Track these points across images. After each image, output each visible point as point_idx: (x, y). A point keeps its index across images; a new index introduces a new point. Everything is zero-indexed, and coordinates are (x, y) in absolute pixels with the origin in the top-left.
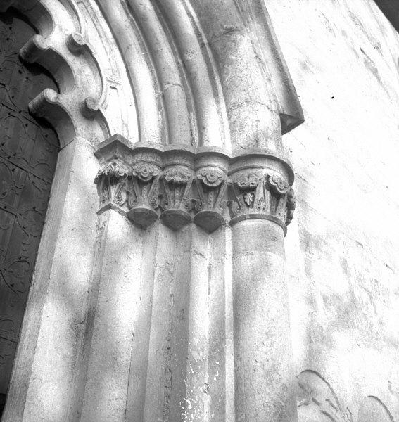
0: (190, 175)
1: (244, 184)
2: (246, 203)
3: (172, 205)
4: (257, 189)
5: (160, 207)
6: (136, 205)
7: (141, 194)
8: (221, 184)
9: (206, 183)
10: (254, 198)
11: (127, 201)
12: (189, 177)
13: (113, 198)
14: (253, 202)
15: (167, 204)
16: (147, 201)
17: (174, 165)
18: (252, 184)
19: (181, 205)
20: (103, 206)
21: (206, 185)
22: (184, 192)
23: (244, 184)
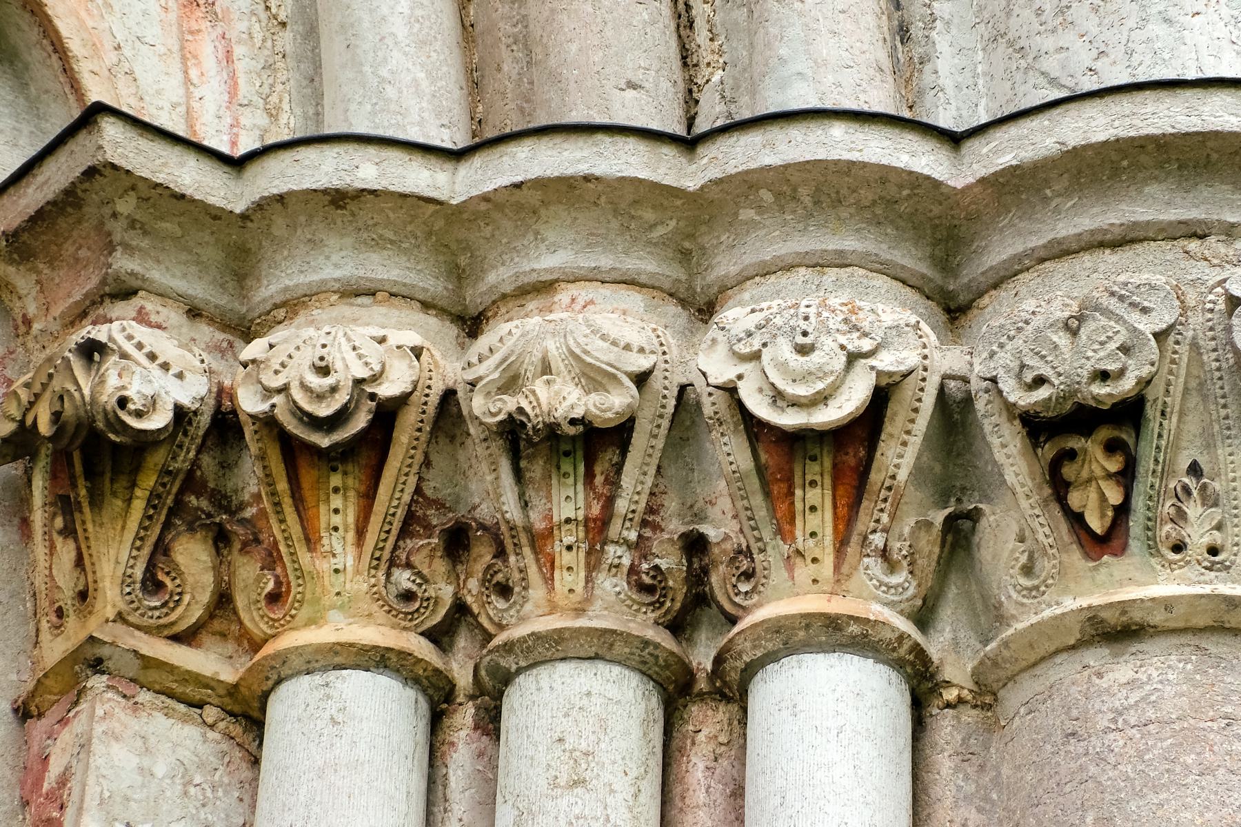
0: (643, 363)
1: (1040, 381)
2: (1076, 520)
3: (537, 592)
4: (1151, 412)
5: (460, 609)
6: (289, 623)
7: (311, 542)
8: (881, 397)
9: (760, 407)
10: (1127, 477)
11: (223, 600)
12: (641, 379)
13: (110, 597)
14: (1123, 511)
15: (504, 591)
16: (358, 585)
17: (543, 288)
18: (1104, 376)
19: (610, 585)
20: (55, 649)
21: (762, 424)
22: (614, 482)
23: (1040, 381)
